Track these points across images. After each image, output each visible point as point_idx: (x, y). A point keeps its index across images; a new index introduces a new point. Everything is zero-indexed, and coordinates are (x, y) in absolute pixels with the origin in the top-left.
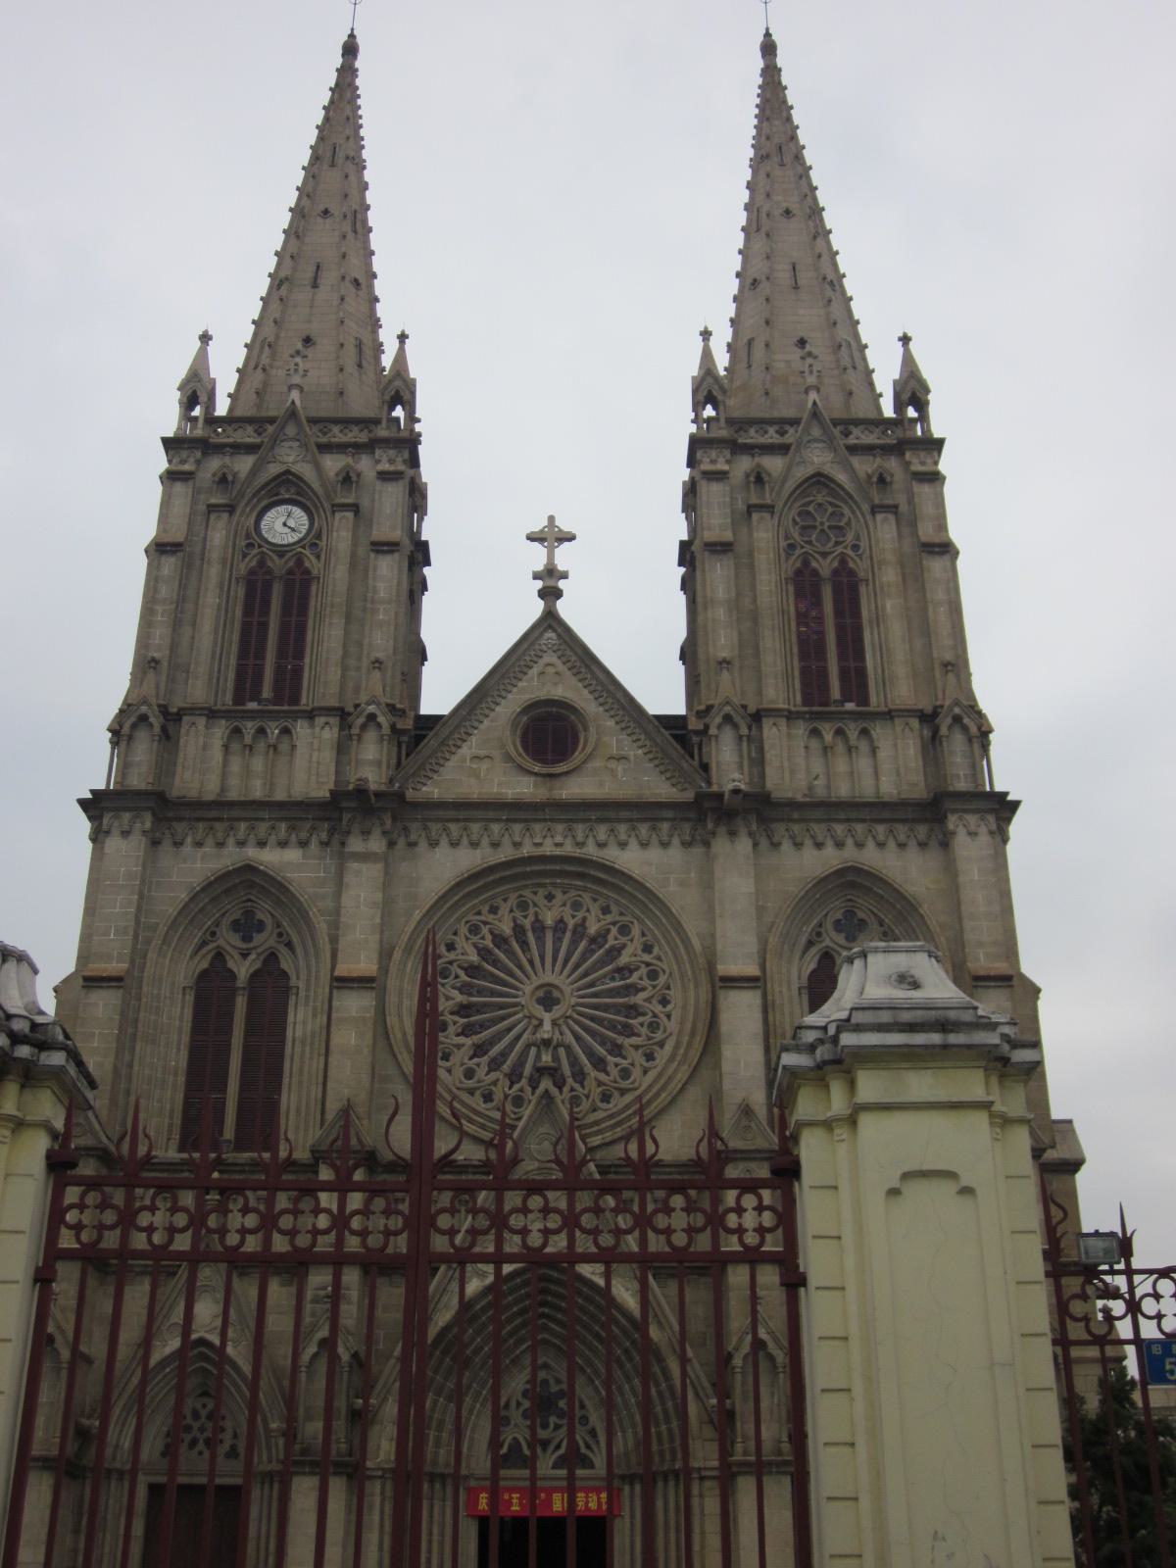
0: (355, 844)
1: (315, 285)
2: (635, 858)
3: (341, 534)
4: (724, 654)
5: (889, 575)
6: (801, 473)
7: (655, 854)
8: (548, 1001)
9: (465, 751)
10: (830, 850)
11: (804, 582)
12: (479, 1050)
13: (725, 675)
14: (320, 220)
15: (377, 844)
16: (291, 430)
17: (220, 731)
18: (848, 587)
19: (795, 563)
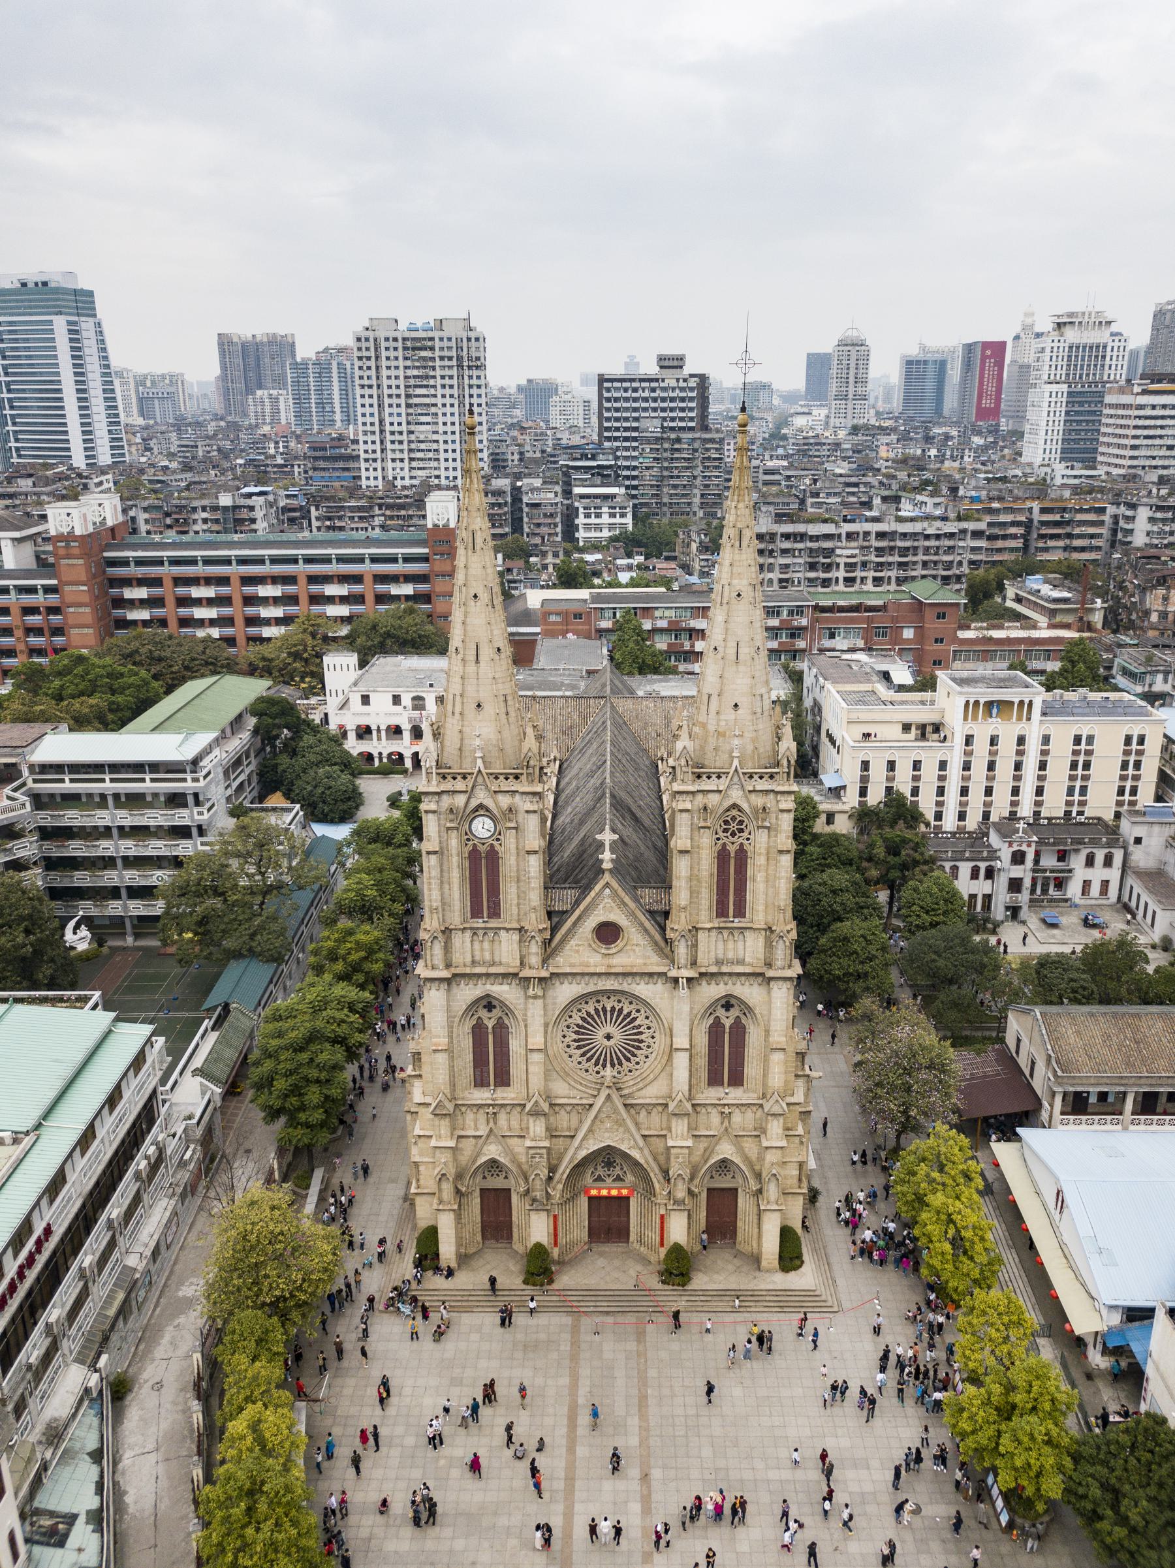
0: (531, 992)
1: (477, 661)
2: (642, 989)
3: (510, 839)
4: (683, 903)
5: (761, 860)
6: (726, 804)
7: (651, 986)
8: (608, 1037)
9: (573, 942)
10: (722, 985)
11: (722, 857)
12: (583, 1055)
13: (683, 915)
14: (472, 603)
15: (540, 993)
16: (480, 779)
17: (468, 934)
18: (742, 856)
19: (719, 847)
